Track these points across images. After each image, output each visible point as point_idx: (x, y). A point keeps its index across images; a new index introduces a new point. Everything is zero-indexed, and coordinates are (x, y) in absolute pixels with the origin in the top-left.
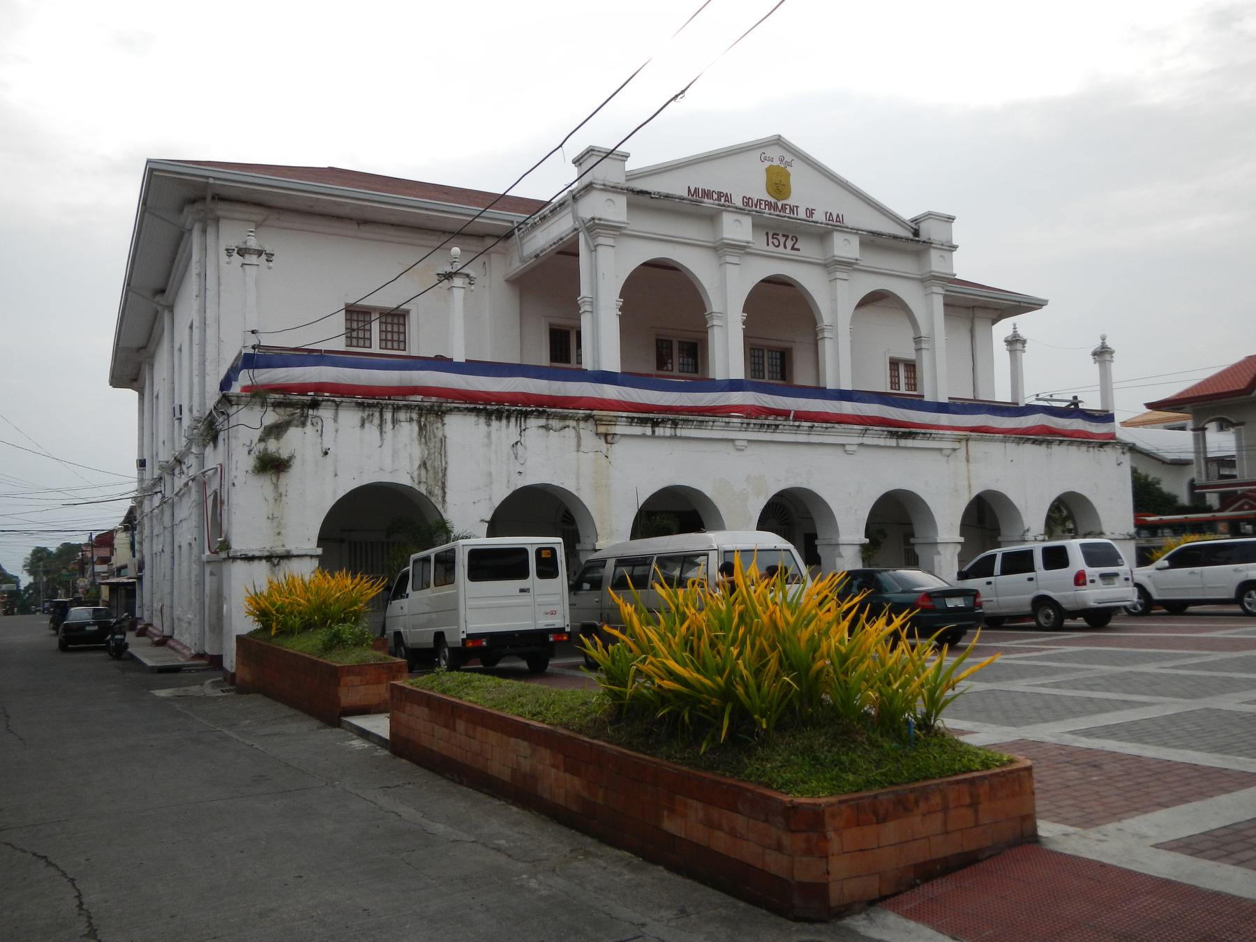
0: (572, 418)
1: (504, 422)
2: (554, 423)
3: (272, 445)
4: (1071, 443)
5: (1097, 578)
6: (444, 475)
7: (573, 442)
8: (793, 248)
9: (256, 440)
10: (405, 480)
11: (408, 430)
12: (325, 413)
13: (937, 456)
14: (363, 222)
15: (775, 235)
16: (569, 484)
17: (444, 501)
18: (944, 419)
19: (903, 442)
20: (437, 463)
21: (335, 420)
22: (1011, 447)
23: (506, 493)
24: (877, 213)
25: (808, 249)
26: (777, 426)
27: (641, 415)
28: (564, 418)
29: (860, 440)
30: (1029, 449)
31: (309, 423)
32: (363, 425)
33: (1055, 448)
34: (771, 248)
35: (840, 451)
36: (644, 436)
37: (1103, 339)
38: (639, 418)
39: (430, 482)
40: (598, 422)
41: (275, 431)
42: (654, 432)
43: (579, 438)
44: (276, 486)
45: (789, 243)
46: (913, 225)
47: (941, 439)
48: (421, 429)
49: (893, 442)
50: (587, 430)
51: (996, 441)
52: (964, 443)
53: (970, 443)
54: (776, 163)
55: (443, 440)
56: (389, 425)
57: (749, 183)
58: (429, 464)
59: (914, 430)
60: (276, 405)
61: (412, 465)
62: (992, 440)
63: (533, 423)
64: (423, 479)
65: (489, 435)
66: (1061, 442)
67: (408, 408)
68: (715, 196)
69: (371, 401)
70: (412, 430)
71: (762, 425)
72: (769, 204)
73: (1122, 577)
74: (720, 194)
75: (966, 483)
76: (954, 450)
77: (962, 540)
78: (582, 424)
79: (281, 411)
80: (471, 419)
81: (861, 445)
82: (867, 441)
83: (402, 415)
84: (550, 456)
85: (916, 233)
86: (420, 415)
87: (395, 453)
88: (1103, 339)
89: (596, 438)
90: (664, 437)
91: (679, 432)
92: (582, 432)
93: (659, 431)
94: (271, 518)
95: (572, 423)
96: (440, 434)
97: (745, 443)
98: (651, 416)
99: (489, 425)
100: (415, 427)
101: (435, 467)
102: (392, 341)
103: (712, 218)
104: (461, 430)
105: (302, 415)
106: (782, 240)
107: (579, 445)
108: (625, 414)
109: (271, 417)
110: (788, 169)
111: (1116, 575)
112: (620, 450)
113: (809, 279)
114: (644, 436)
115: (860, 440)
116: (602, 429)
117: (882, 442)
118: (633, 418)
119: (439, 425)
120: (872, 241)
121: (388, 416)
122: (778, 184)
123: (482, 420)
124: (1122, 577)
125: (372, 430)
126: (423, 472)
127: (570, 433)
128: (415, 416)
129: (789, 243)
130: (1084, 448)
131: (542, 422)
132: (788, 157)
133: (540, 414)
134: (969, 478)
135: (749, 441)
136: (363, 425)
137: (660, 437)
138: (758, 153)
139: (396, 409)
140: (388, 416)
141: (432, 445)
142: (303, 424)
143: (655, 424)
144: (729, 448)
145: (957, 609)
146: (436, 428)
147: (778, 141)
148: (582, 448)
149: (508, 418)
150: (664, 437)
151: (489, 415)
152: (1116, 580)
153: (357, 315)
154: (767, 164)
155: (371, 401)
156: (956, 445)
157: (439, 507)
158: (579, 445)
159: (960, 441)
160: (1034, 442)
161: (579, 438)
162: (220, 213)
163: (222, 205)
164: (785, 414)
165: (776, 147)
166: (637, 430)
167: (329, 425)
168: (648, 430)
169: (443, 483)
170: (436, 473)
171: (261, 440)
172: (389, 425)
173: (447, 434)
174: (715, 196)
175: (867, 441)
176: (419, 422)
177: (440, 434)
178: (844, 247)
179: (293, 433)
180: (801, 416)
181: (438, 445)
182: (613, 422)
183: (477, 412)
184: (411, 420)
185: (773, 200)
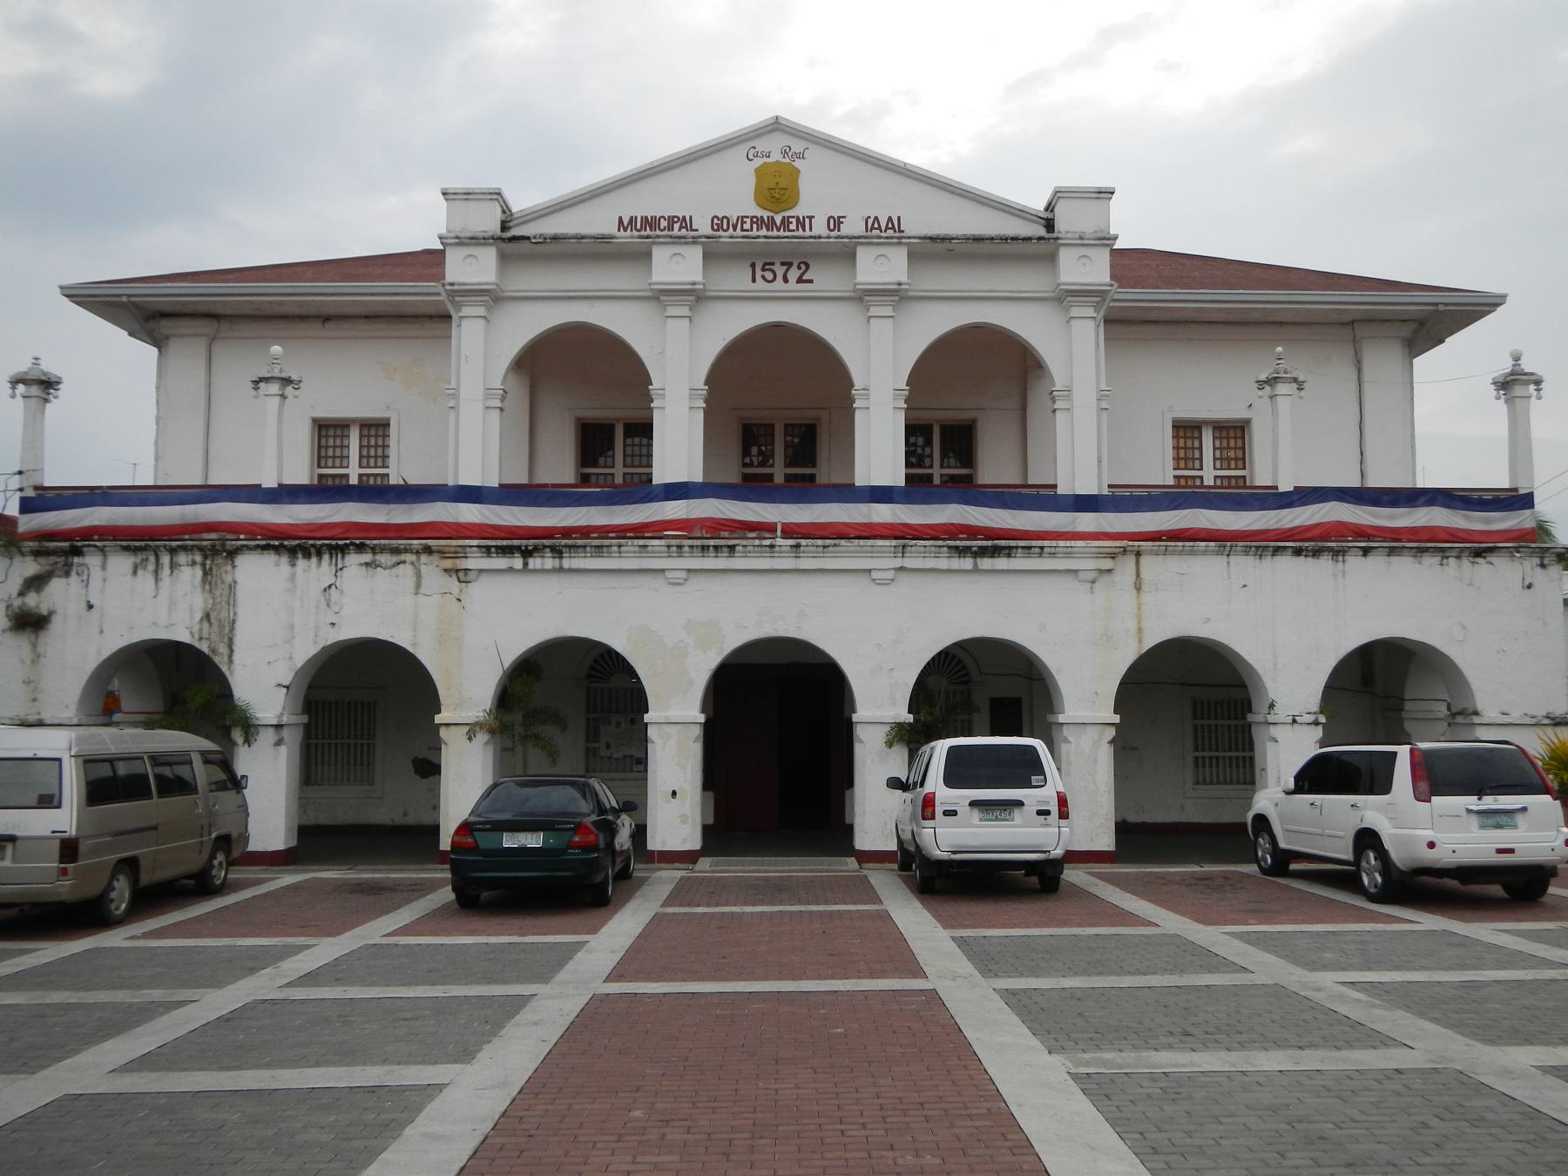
0: (406, 551)
1: (314, 560)
2: (384, 558)
3: (32, 600)
5: (963, 809)
6: (232, 629)
7: (411, 582)
8: (800, 280)
9: (15, 593)
10: (183, 636)
11: (189, 576)
12: (92, 560)
13: (1068, 582)
14: (327, 319)
15: (767, 266)
16: (402, 639)
17: (231, 661)
18: (1087, 521)
19: (986, 563)
20: (224, 615)
21: (104, 568)
23: (312, 650)
24: (970, 204)
25: (825, 279)
26: (732, 548)
27: (499, 543)
28: (395, 551)
29: (898, 563)
30: (1286, 563)
31: (73, 573)
32: (135, 572)
33: (1354, 562)
34: (760, 283)
35: (863, 581)
36: (511, 570)
37: (1517, 359)
38: (497, 547)
39: (214, 637)
40: (442, 553)
41: (35, 583)
42: (526, 564)
43: (419, 576)
44: (34, 646)
45: (794, 274)
46: (1045, 215)
48: (205, 573)
49: (967, 563)
50: (431, 569)
51: (1205, 553)
52: (1131, 559)
53: (1144, 560)
54: (776, 157)
55: (232, 587)
56: (166, 571)
57: (731, 194)
58: (213, 616)
60: (37, 554)
61: (192, 617)
62: (1192, 553)
63: (353, 560)
64: (205, 635)
65: (293, 578)
66: (1366, 552)
67: (185, 549)
68: (664, 224)
69: (137, 544)
70: (194, 576)
71: (704, 548)
72: (759, 222)
73: (1030, 808)
74: (672, 220)
75: (1132, 626)
76: (1109, 571)
77: (1117, 719)
78: (424, 558)
79: (42, 560)
80: (270, 558)
81: (901, 568)
82: (909, 563)
83: (182, 558)
84: (373, 602)
85: (1050, 225)
86: (205, 557)
87: (172, 604)
88: (1517, 359)
89: (445, 577)
90: (543, 571)
91: (566, 563)
92: (423, 568)
93: (535, 563)
94: (27, 682)
95: (409, 557)
96: (229, 579)
97: (683, 575)
98: (515, 542)
99: (294, 565)
100: (199, 572)
101: (220, 619)
102: (376, 457)
103: (641, 256)
104: (257, 574)
105: (66, 564)
106: (780, 271)
107: (418, 585)
108: (475, 542)
109: (31, 567)
110: (798, 164)
111: (1020, 804)
112: (482, 593)
113: (831, 324)
114: (511, 570)
115: (898, 563)
116: (448, 564)
117: (943, 563)
118: (488, 548)
119: (229, 568)
120: (936, 250)
121: (165, 559)
122: (777, 189)
123: (285, 559)
124: (1030, 808)
125: (146, 578)
126: (206, 625)
127: (406, 571)
128: (198, 558)
129: (794, 274)
130: (1430, 561)
131: (367, 557)
132: (797, 146)
133: (361, 548)
135: (689, 571)
136: (135, 572)
137: (535, 571)
138: (745, 147)
139: (173, 551)
140: (165, 559)
141: (218, 593)
142: (67, 574)
143: (527, 554)
144: (659, 581)
145: (523, 851)
146: (226, 573)
147: (776, 126)
148: (423, 590)
149: (319, 554)
150: (543, 571)
151: (292, 552)
152: (1017, 813)
153: (328, 431)
154: (758, 162)
155: (137, 544)
156: (1107, 564)
157: (224, 669)
158: (418, 585)
159: (1113, 556)
160: (1298, 552)
161: (419, 576)
162: (165, 331)
163: (164, 322)
164: (766, 528)
165: (777, 134)
166: (500, 562)
167: (96, 573)
168: (518, 562)
169: (231, 640)
170: (221, 627)
171: (21, 594)
172: (166, 571)
173: (239, 578)
174: (664, 224)
175: (909, 563)
176: (203, 565)
177: (229, 579)
178: (881, 267)
179: (56, 585)
180: (791, 531)
181: (226, 592)
182: (461, 553)
183: (277, 550)
184: (194, 563)
185: (766, 214)
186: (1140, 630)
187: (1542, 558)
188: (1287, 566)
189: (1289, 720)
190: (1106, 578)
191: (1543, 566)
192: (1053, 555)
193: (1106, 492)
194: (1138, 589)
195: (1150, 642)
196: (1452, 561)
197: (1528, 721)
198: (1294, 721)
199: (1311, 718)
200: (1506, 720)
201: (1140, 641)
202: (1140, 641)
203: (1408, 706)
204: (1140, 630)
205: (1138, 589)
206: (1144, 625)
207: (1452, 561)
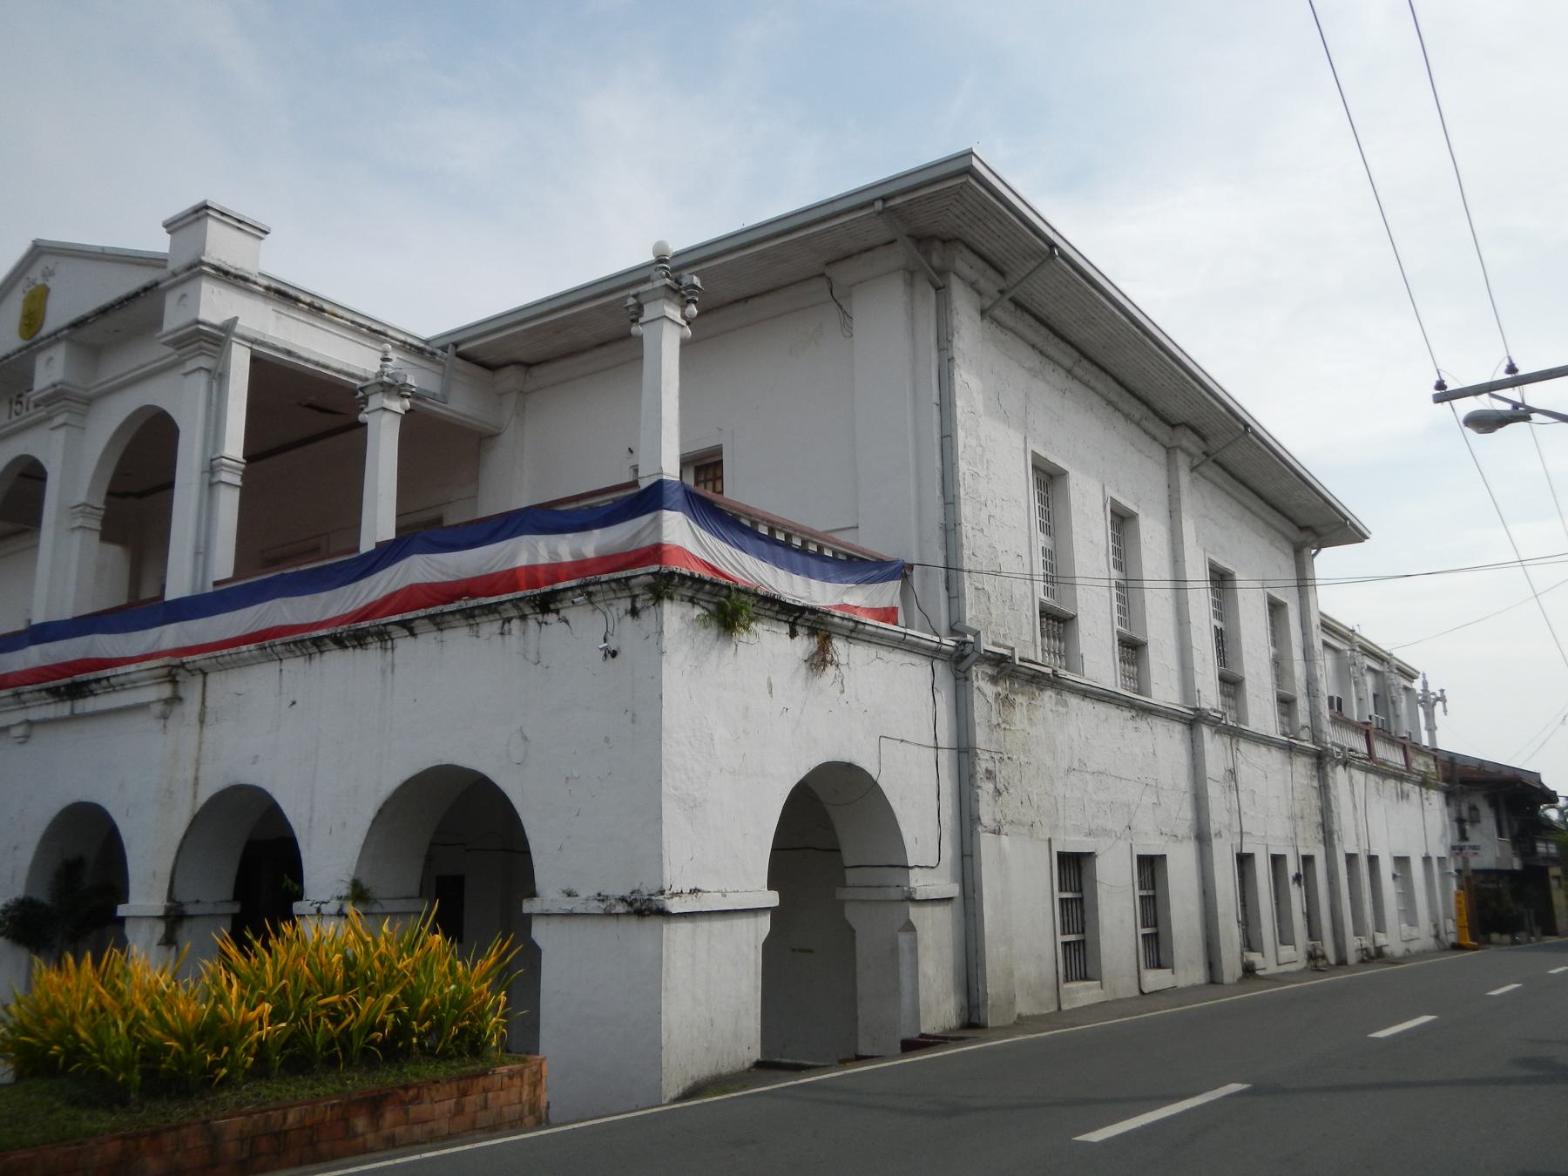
4: (438, 622)
22: (295, 666)
30: (335, 660)
33: (404, 646)
47: (134, 685)
49: (64, 709)
52: (199, 679)
53: (213, 679)
59: (79, 678)
75: (190, 775)
81: (30, 723)
82: (35, 714)
130: (489, 628)
134: (198, 762)
186: (196, 778)
187: (634, 597)
188: (342, 670)
189: (314, 911)
190: (178, 710)
191: (634, 612)
192: (113, 689)
193: (210, 589)
194: (202, 722)
195: (204, 796)
196: (515, 623)
197: (595, 907)
198: (319, 910)
199: (333, 907)
200: (567, 905)
201: (195, 797)
202: (195, 797)
203: (852, 876)
204: (196, 778)
205: (202, 722)
206: (201, 773)
207: (515, 623)
